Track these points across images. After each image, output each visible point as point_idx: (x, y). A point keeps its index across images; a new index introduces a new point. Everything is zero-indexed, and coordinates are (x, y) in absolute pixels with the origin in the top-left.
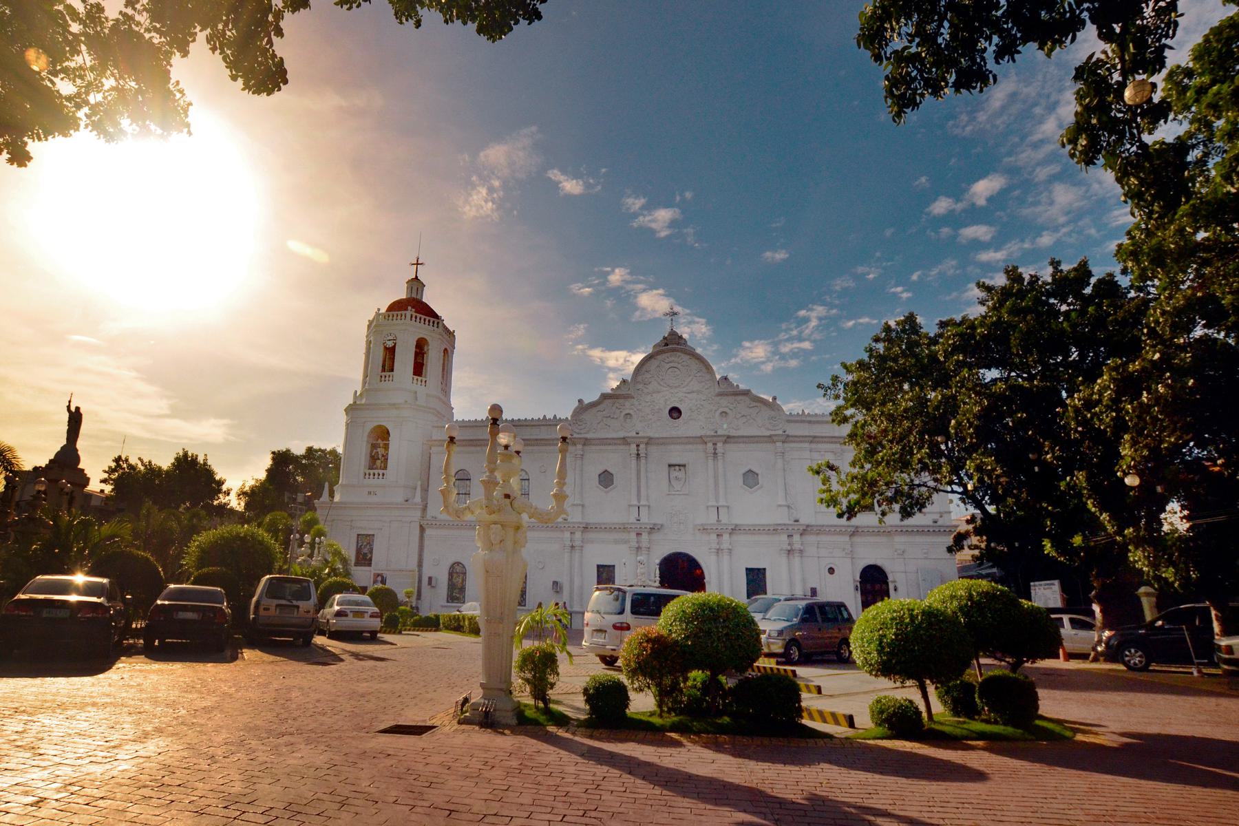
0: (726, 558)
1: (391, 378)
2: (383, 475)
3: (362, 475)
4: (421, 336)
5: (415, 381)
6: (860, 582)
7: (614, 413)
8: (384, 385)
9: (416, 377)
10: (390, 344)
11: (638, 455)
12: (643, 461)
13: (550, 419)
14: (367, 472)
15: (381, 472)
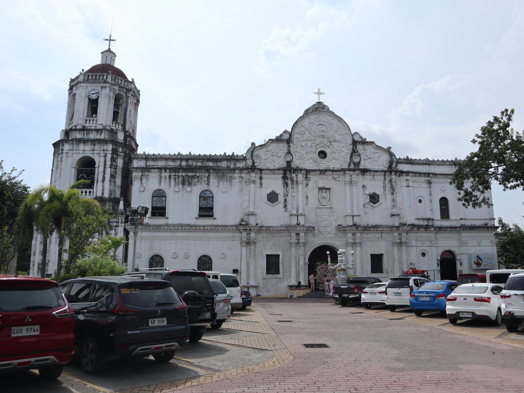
2: (90, 192)
7: (278, 153)
10: (94, 97)
13: (229, 156)
15: (88, 190)
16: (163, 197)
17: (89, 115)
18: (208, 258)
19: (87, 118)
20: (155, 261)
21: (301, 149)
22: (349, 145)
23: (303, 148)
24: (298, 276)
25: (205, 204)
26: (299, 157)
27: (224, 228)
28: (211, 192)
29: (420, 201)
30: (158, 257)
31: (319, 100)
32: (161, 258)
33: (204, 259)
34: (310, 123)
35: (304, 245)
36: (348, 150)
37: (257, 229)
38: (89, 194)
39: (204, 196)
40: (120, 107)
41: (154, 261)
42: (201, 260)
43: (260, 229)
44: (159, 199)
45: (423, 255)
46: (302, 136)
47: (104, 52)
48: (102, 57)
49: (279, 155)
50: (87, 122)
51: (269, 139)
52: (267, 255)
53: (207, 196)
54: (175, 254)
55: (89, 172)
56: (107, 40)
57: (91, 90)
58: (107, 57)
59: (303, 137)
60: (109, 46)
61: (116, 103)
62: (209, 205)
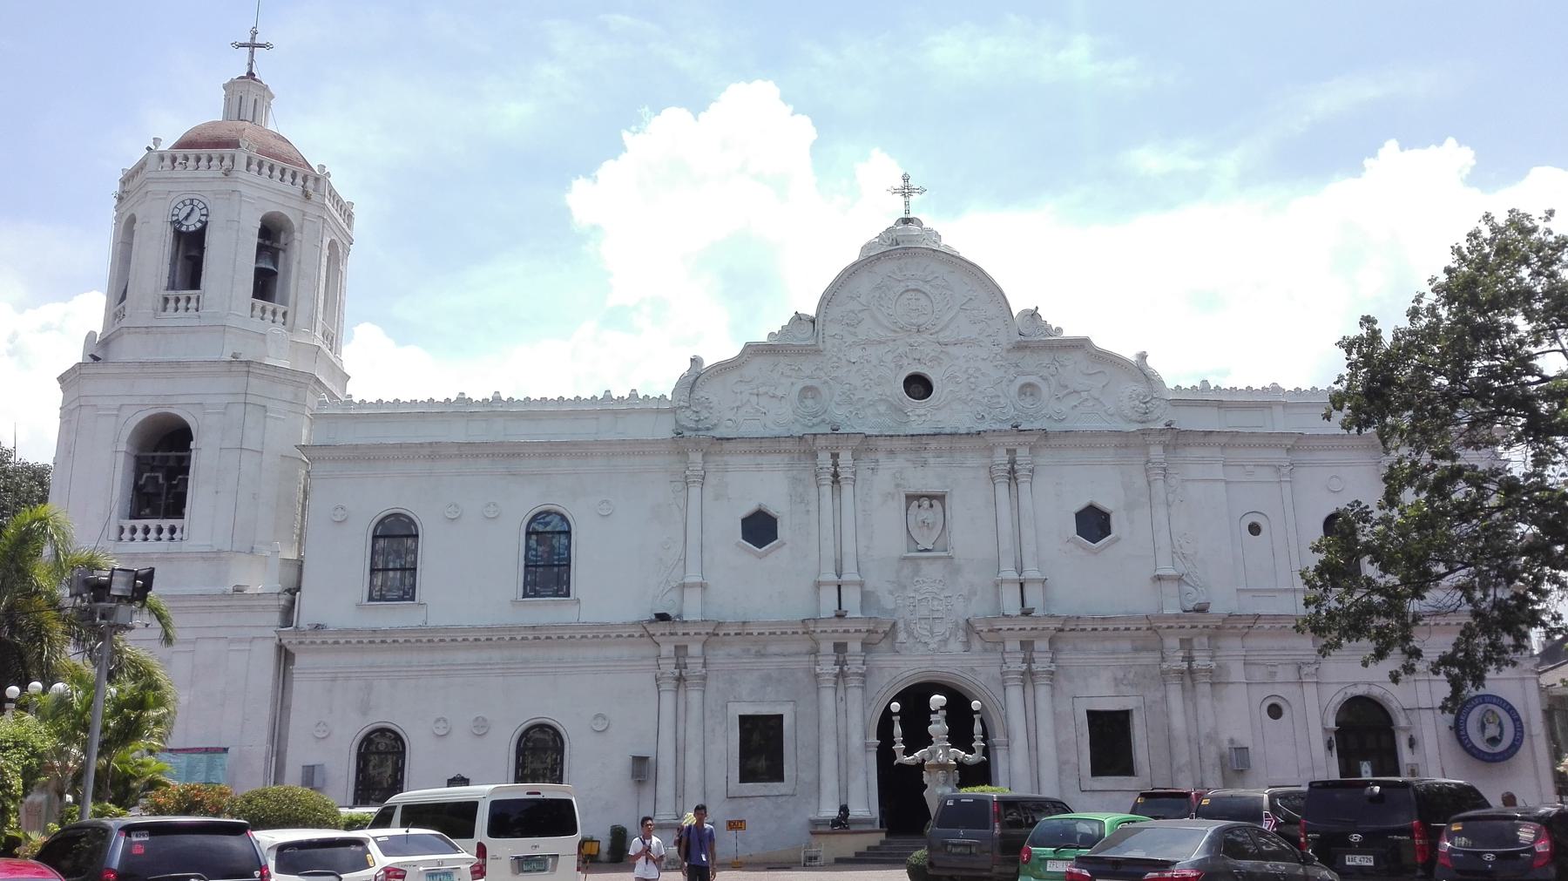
0: (1043, 692)
1: (193, 304)
2: (173, 530)
3: (114, 534)
4: (271, 208)
5: (258, 312)
6: (1336, 732)
8: (172, 318)
9: (259, 303)
10: (192, 225)
11: (836, 475)
12: (847, 490)
13: (621, 399)
14: (128, 524)
15: (166, 524)
16: (407, 536)
17: (177, 280)
18: (551, 732)
19: (166, 293)
20: (377, 748)
21: (849, 371)
22: (1004, 354)
23: (855, 368)
24: (844, 790)
25: (546, 555)
26: (844, 397)
27: (601, 634)
28: (563, 518)
29: (1255, 529)
30: (389, 734)
31: (907, 212)
32: (398, 738)
33: (539, 735)
34: (878, 288)
35: (864, 682)
36: (1003, 369)
37: (707, 633)
38: (169, 536)
39: (540, 528)
40: (281, 254)
41: (373, 748)
42: (528, 740)
43: (715, 633)
44: (395, 544)
45: (1275, 711)
46: (851, 329)
47: (232, 82)
48: (228, 100)
49: (779, 393)
50: (168, 306)
51: (748, 346)
52: (740, 716)
53: (549, 529)
54: (441, 724)
55: (171, 463)
56: (243, 45)
57: (183, 202)
58: (241, 97)
59: (855, 334)
60: (251, 65)
61: (267, 243)
62: (556, 557)
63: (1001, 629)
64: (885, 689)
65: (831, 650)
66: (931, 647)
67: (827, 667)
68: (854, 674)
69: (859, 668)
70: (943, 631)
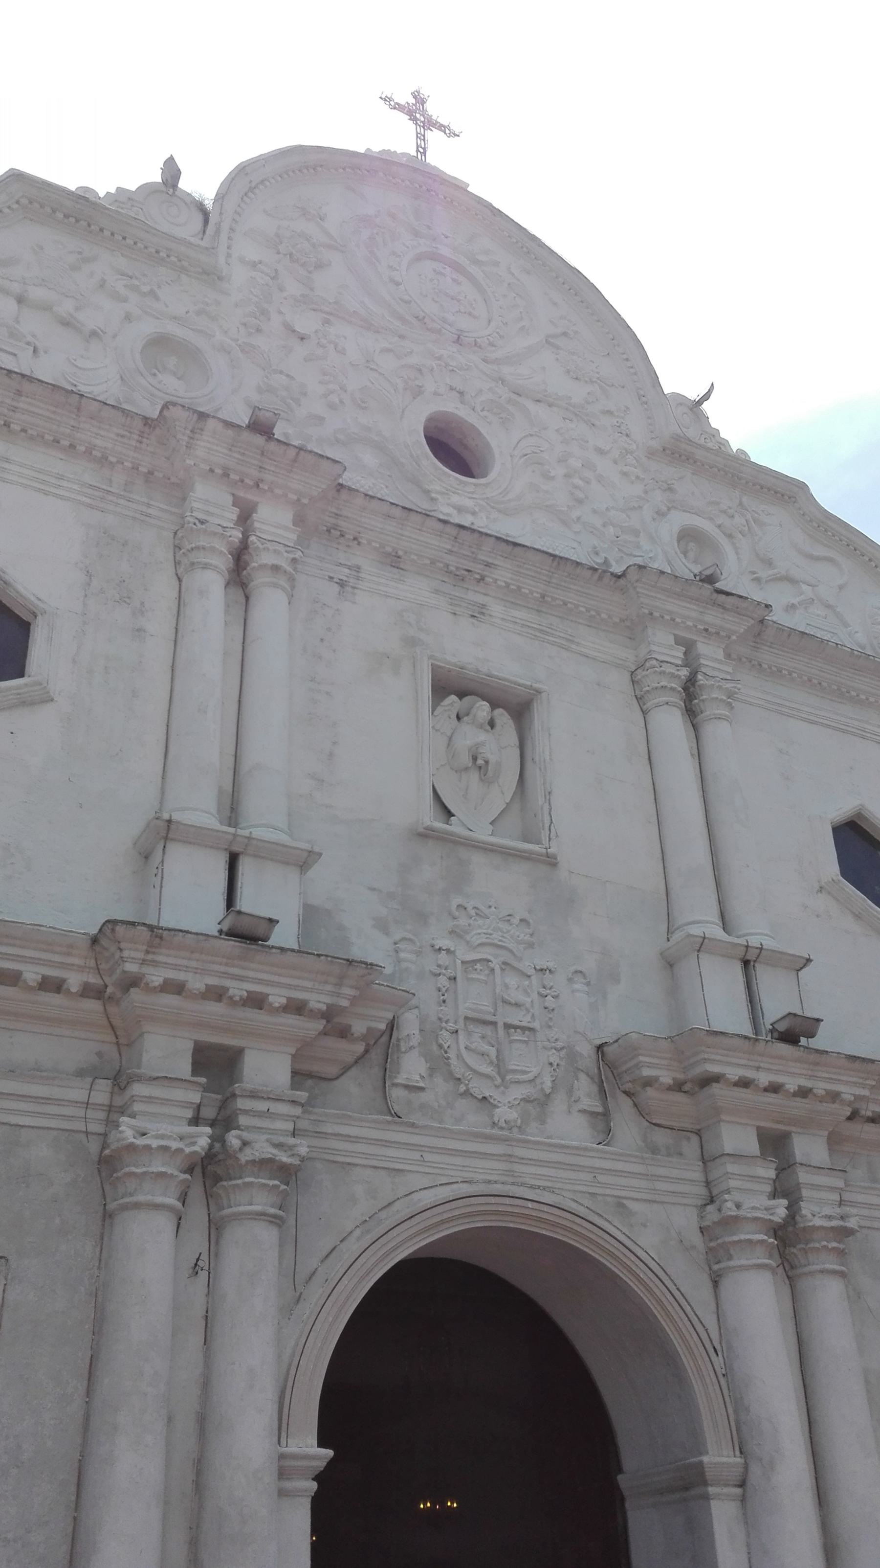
63: (716, 1078)
64: (353, 1247)
65: (184, 1068)
66: (504, 1113)
67: (165, 1128)
68: (265, 1164)
69: (279, 1146)
70: (535, 1071)
